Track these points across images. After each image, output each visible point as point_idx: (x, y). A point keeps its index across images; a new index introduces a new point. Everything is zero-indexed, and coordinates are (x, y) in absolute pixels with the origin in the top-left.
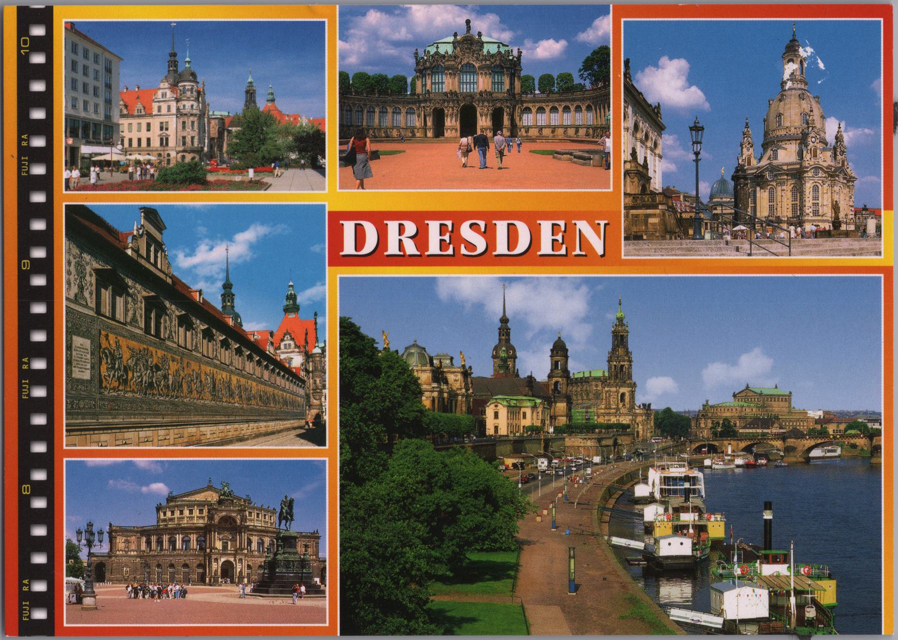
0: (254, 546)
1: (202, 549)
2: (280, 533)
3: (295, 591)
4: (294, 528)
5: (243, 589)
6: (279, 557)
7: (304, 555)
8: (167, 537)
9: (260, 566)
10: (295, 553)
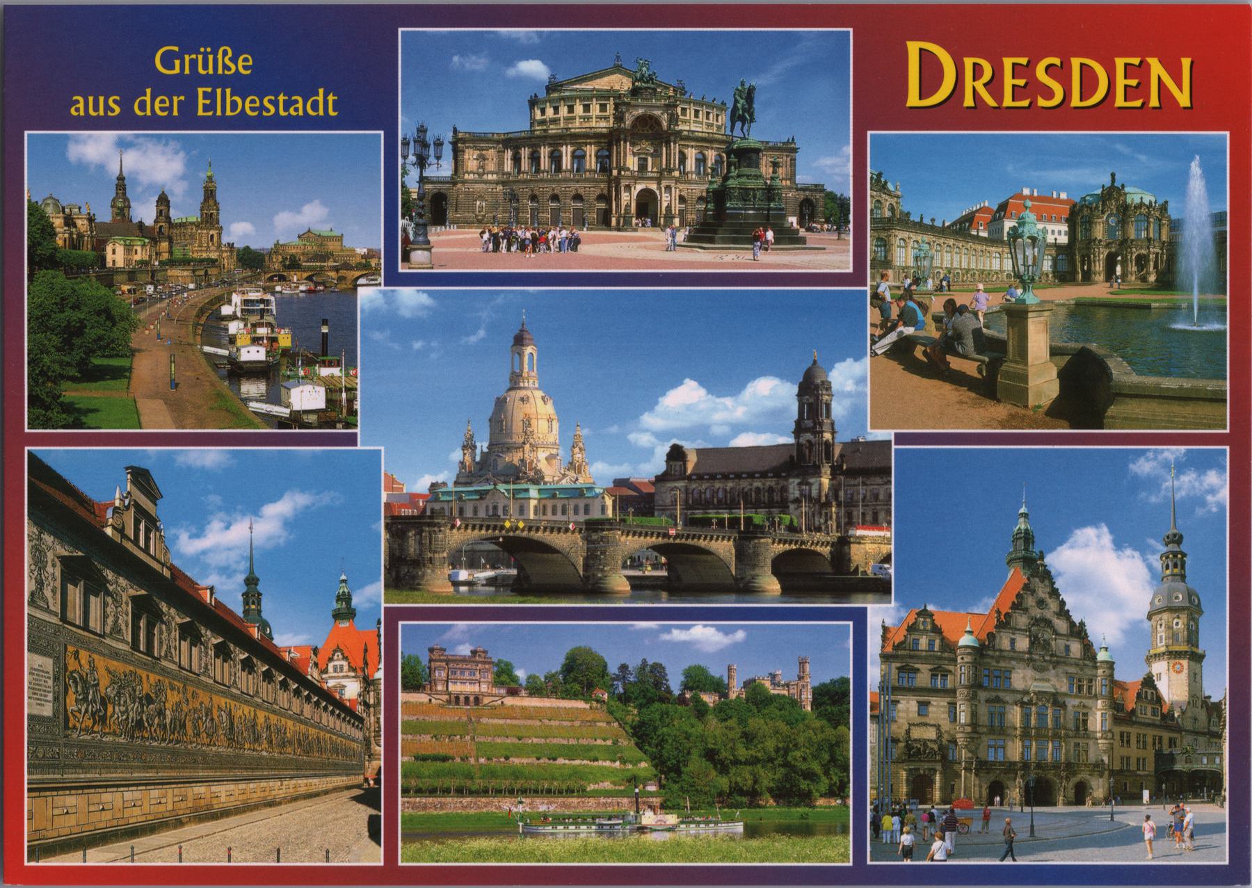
0: (690, 164)
1: (605, 169)
2: (732, 142)
3: (757, 238)
4: (755, 136)
5: (673, 236)
7: (772, 179)
9: (700, 199)
10: (758, 177)
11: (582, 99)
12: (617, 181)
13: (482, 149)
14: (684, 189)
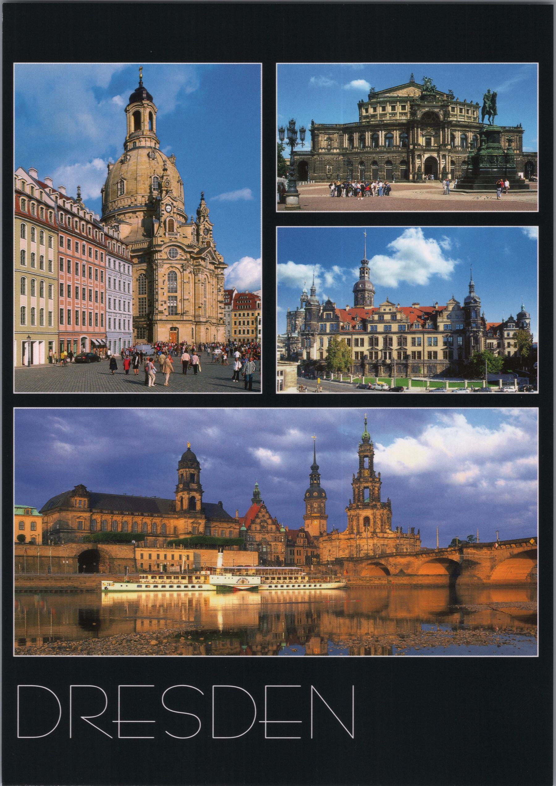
0: (458, 141)
1: (405, 145)
3: (499, 186)
5: (448, 185)
6: (483, 152)
7: (508, 149)
8: (370, 133)
9: (464, 162)
11: (391, 102)
12: (413, 151)
13: (329, 134)
14: (455, 156)
